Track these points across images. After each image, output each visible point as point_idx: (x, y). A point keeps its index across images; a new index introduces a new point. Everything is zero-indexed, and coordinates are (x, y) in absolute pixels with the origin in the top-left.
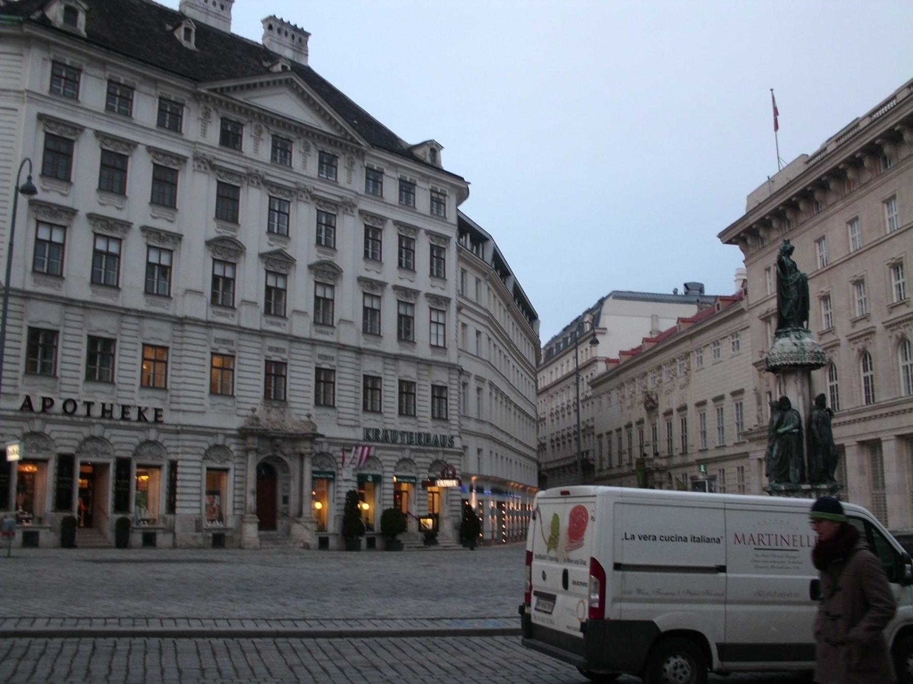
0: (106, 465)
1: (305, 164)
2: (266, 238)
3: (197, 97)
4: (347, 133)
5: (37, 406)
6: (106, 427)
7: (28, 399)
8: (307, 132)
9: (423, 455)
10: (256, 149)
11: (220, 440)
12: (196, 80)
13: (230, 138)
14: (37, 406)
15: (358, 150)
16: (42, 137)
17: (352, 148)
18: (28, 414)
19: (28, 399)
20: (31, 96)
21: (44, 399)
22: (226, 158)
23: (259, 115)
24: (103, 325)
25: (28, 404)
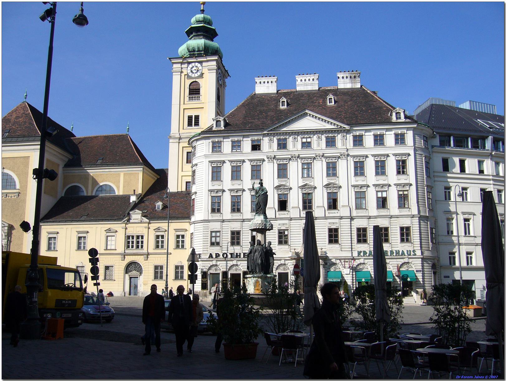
0: (240, 274)
1: (319, 144)
2: (301, 180)
3: (264, 135)
4: (338, 125)
5: (214, 256)
6: (239, 261)
7: (211, 254)
8: (317, 132)
9: (395, 260)
10: (294, 146)
11: (282, 262)
12: (263, 129)
13: (282, 145)
14: (214, 256)
15: (344, 130)
16: (211, 168)
17: (341, 130)
18: (211, 259)
19: (211, 254)
20: (206, 156)
21: (216, 254)
22: (282, 154)
23: (292, 133)
24: (236, 226)
25: (211, 256)
